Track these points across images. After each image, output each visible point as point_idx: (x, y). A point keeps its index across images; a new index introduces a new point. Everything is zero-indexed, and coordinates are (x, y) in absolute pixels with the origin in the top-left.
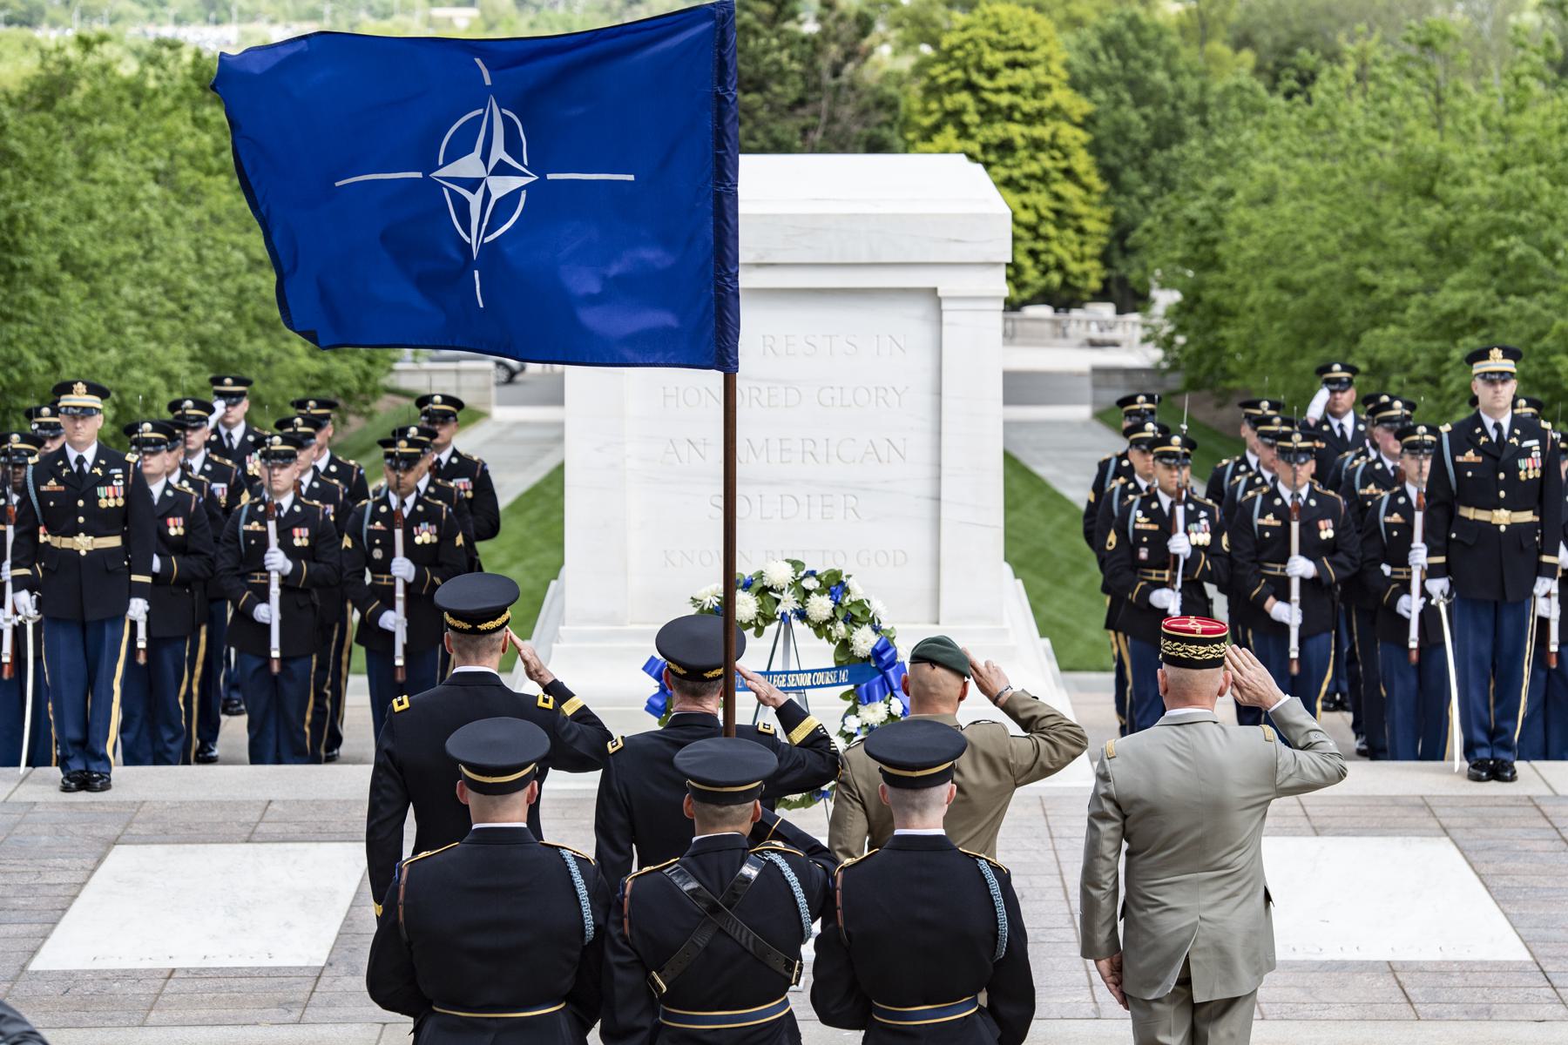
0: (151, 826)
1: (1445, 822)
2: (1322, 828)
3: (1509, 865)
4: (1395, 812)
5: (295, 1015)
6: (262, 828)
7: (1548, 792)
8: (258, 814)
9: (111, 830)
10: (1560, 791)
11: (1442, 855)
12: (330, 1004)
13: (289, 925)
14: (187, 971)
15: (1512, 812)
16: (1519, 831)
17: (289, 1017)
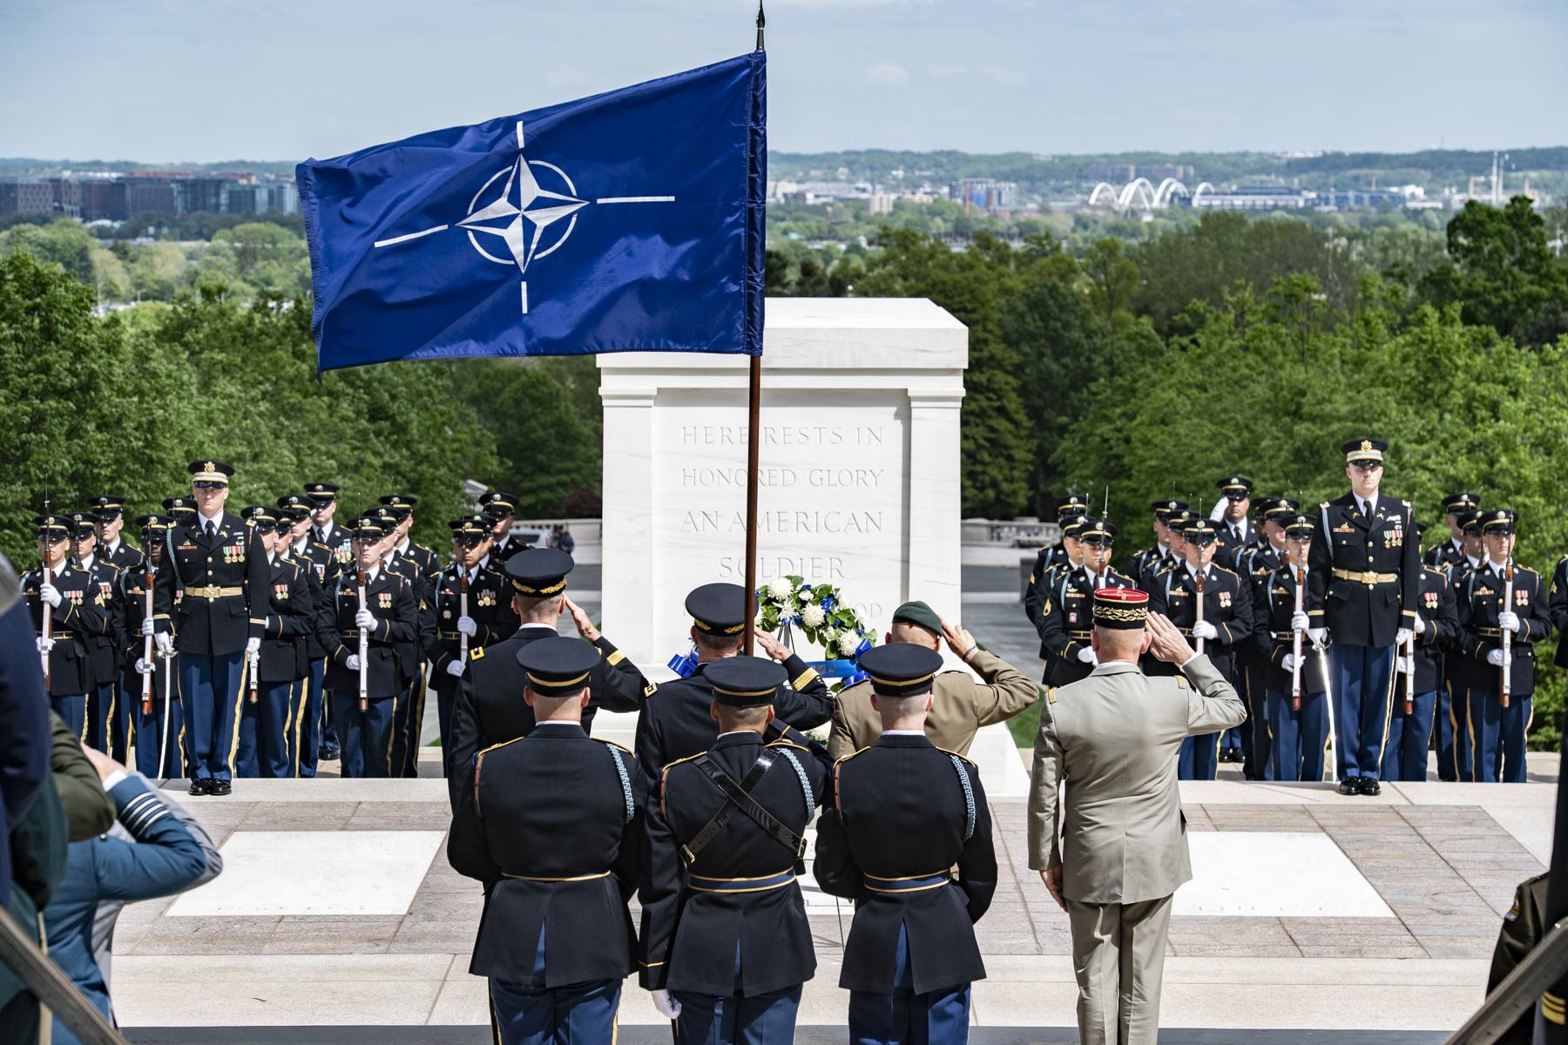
0: (264, 819)
1: (1321, 822)
2: (1222, 826)
3: (1376, 852)
4: (1281, 815)
5: (383, 946)
6: (353, 820)
7: (1407, 803)
8: (350, 811)
9: (231, 821)
10: (1415, 802)
11: (1321, 845)
12: (410, 940)
13: (376, 887)
14: (294, 917)
15: (1378, 815)
16: (1383, 829)
17: (377, 949)
